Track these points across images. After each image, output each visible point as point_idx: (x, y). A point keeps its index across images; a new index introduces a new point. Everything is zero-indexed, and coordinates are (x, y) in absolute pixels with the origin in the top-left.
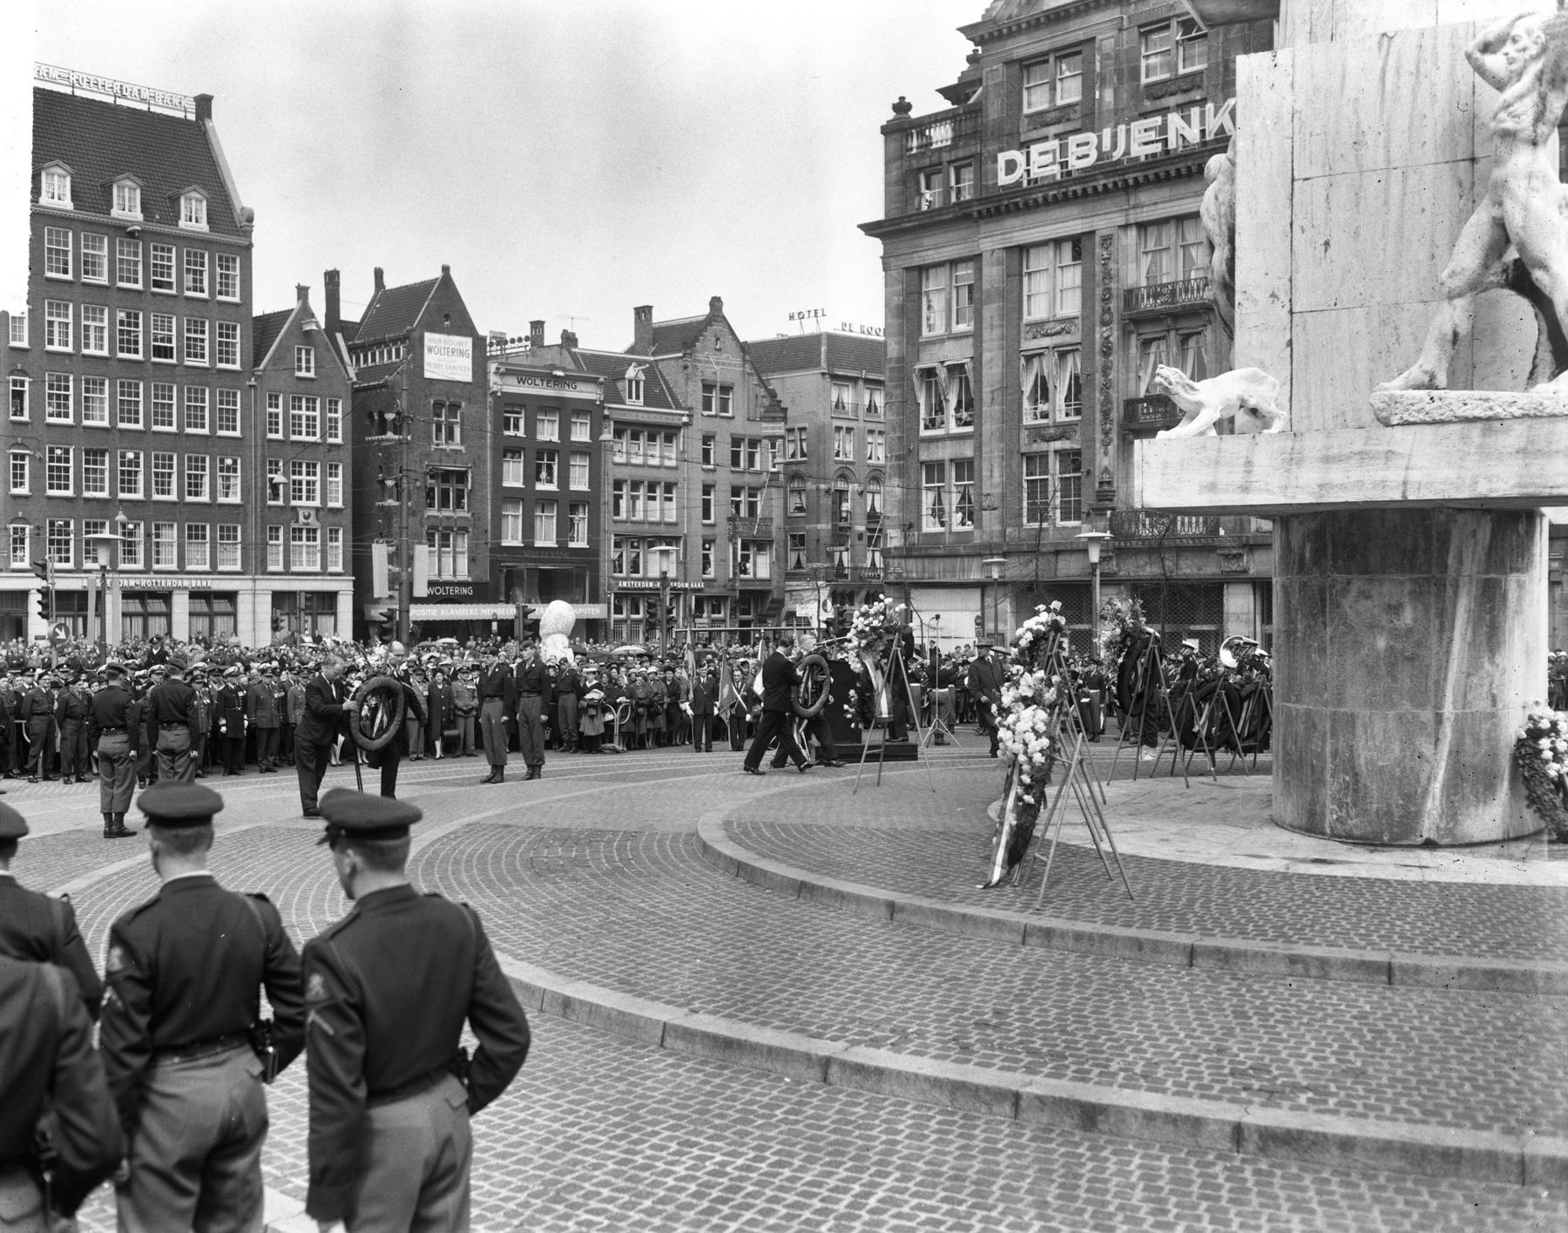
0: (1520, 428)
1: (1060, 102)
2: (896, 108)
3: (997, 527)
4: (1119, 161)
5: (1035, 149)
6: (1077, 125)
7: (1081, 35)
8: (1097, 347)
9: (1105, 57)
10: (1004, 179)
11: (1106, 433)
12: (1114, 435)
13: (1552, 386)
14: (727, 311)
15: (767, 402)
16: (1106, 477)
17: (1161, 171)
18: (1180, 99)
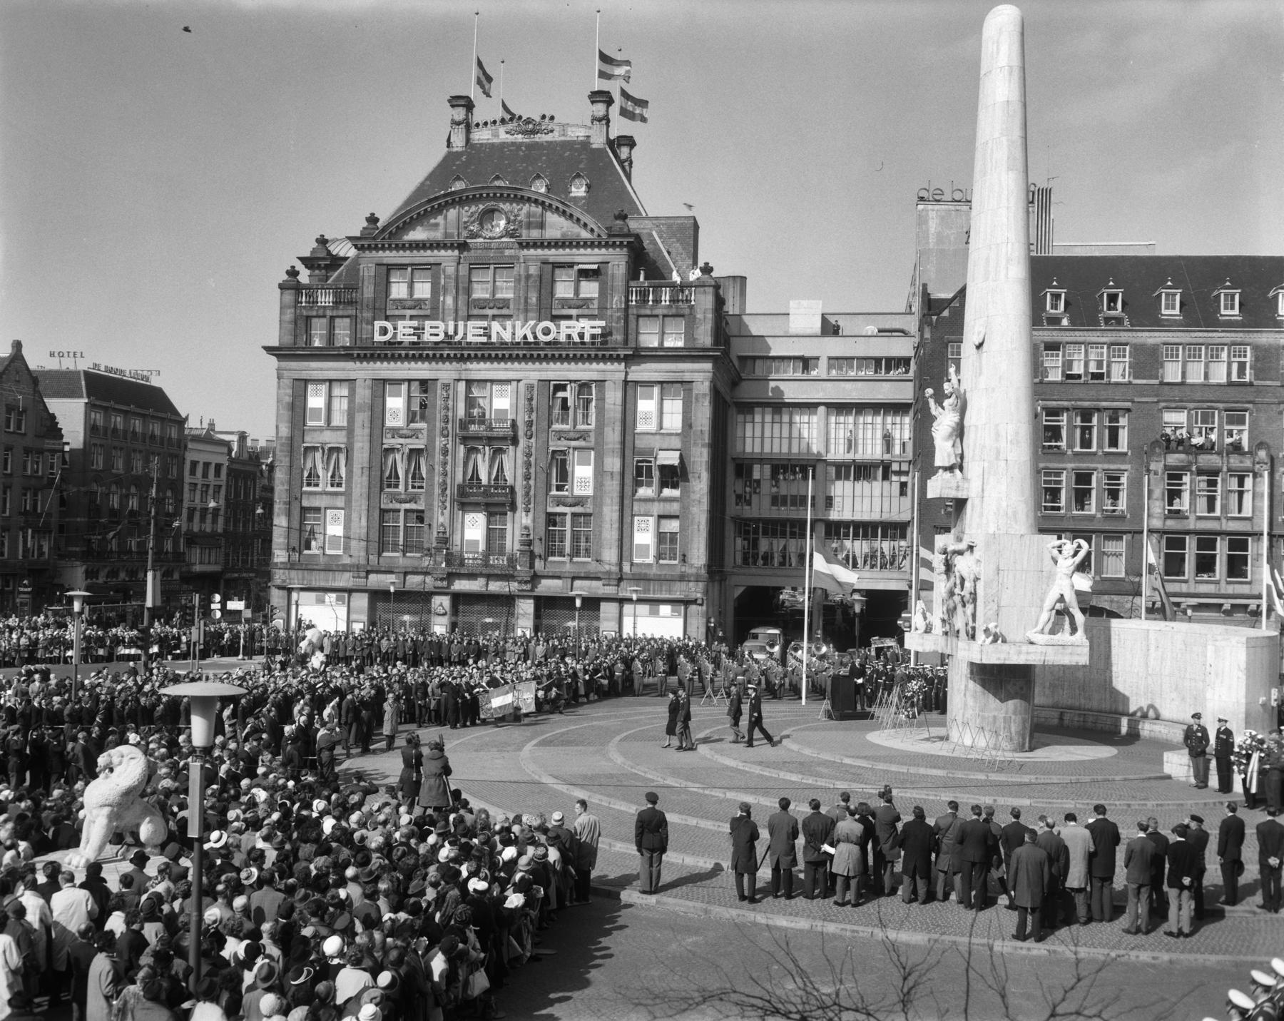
1: (416, 296)
2: (287, 272)
3: (363, 554)
4: (460, 343)
5: (400, 324)
6: (428, 312)
7: (432, 260)
8: (437, 450)
9: (449, 277)
10: (378, 338)
11: (443, 502)
12: (448, 504)
13: (1073, 638)
14: (25, 352)
15: (48, 423)
16: (442, 529)
17: (486, 353)
18: (495, 312)
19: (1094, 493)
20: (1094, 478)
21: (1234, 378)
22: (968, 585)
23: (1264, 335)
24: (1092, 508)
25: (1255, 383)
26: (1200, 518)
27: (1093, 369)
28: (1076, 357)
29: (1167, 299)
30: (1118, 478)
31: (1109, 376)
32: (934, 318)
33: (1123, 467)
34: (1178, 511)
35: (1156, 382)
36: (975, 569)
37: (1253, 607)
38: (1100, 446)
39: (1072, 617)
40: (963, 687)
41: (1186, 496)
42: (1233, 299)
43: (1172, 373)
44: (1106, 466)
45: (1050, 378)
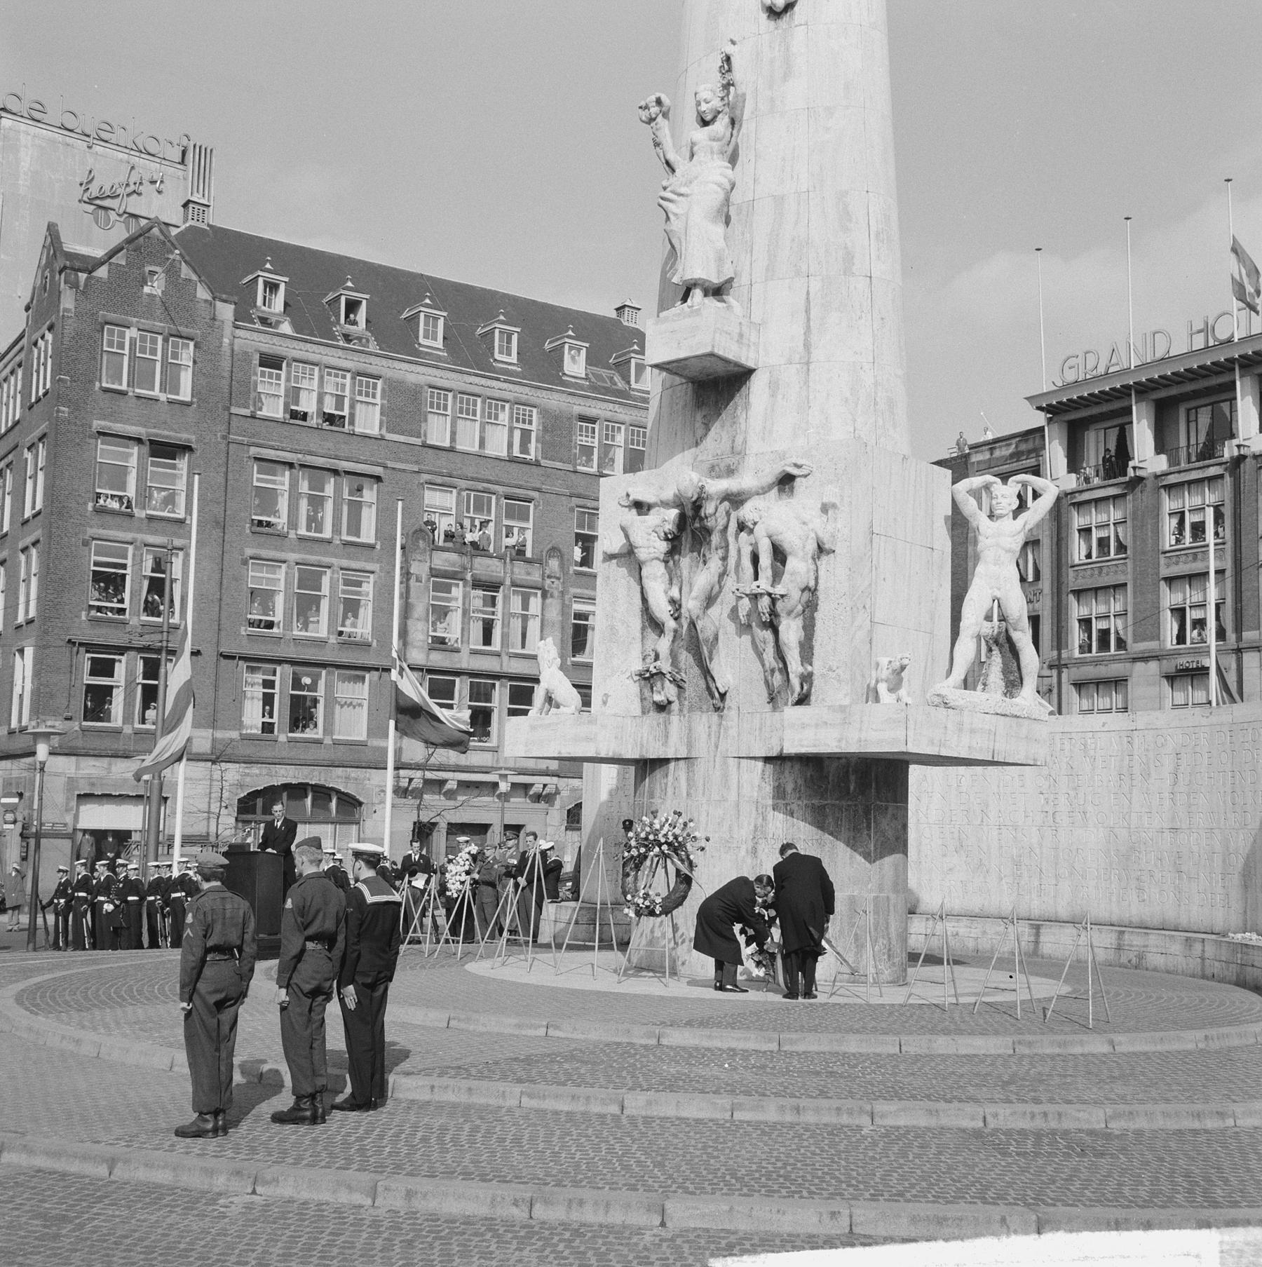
0: (1026, 722)
19: (325, 605)
20: (326, 581)
21: (516, 452)
22: (798, 567)
23: (556, 396)
24: (321, 628)
25: (543, 462)
26: (474, 652)
27: (329, 408)
28: (304, 384)
29: (426, 324)
30: (359, 584)
31: (352, 423)
32: (83, 276)
33: (369, 567)
34: (442, 641)
35: (418, 441)
36: (820, 527)
37: (537, 789)
38: (336, 529)
39: (1012, 651)
40: (745, 832)
41: (455, 619)
42: (509, 341)
43: (437, 431)
44: (345, 563)
45: (264, 413)
